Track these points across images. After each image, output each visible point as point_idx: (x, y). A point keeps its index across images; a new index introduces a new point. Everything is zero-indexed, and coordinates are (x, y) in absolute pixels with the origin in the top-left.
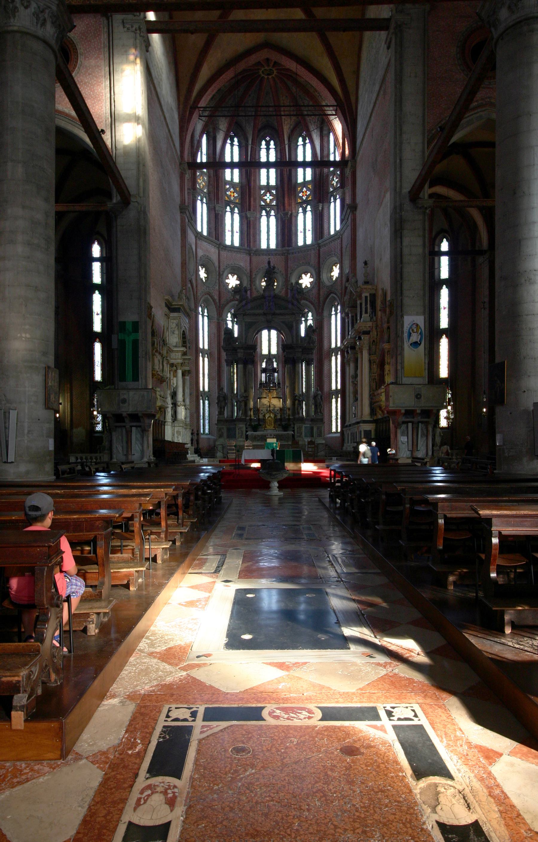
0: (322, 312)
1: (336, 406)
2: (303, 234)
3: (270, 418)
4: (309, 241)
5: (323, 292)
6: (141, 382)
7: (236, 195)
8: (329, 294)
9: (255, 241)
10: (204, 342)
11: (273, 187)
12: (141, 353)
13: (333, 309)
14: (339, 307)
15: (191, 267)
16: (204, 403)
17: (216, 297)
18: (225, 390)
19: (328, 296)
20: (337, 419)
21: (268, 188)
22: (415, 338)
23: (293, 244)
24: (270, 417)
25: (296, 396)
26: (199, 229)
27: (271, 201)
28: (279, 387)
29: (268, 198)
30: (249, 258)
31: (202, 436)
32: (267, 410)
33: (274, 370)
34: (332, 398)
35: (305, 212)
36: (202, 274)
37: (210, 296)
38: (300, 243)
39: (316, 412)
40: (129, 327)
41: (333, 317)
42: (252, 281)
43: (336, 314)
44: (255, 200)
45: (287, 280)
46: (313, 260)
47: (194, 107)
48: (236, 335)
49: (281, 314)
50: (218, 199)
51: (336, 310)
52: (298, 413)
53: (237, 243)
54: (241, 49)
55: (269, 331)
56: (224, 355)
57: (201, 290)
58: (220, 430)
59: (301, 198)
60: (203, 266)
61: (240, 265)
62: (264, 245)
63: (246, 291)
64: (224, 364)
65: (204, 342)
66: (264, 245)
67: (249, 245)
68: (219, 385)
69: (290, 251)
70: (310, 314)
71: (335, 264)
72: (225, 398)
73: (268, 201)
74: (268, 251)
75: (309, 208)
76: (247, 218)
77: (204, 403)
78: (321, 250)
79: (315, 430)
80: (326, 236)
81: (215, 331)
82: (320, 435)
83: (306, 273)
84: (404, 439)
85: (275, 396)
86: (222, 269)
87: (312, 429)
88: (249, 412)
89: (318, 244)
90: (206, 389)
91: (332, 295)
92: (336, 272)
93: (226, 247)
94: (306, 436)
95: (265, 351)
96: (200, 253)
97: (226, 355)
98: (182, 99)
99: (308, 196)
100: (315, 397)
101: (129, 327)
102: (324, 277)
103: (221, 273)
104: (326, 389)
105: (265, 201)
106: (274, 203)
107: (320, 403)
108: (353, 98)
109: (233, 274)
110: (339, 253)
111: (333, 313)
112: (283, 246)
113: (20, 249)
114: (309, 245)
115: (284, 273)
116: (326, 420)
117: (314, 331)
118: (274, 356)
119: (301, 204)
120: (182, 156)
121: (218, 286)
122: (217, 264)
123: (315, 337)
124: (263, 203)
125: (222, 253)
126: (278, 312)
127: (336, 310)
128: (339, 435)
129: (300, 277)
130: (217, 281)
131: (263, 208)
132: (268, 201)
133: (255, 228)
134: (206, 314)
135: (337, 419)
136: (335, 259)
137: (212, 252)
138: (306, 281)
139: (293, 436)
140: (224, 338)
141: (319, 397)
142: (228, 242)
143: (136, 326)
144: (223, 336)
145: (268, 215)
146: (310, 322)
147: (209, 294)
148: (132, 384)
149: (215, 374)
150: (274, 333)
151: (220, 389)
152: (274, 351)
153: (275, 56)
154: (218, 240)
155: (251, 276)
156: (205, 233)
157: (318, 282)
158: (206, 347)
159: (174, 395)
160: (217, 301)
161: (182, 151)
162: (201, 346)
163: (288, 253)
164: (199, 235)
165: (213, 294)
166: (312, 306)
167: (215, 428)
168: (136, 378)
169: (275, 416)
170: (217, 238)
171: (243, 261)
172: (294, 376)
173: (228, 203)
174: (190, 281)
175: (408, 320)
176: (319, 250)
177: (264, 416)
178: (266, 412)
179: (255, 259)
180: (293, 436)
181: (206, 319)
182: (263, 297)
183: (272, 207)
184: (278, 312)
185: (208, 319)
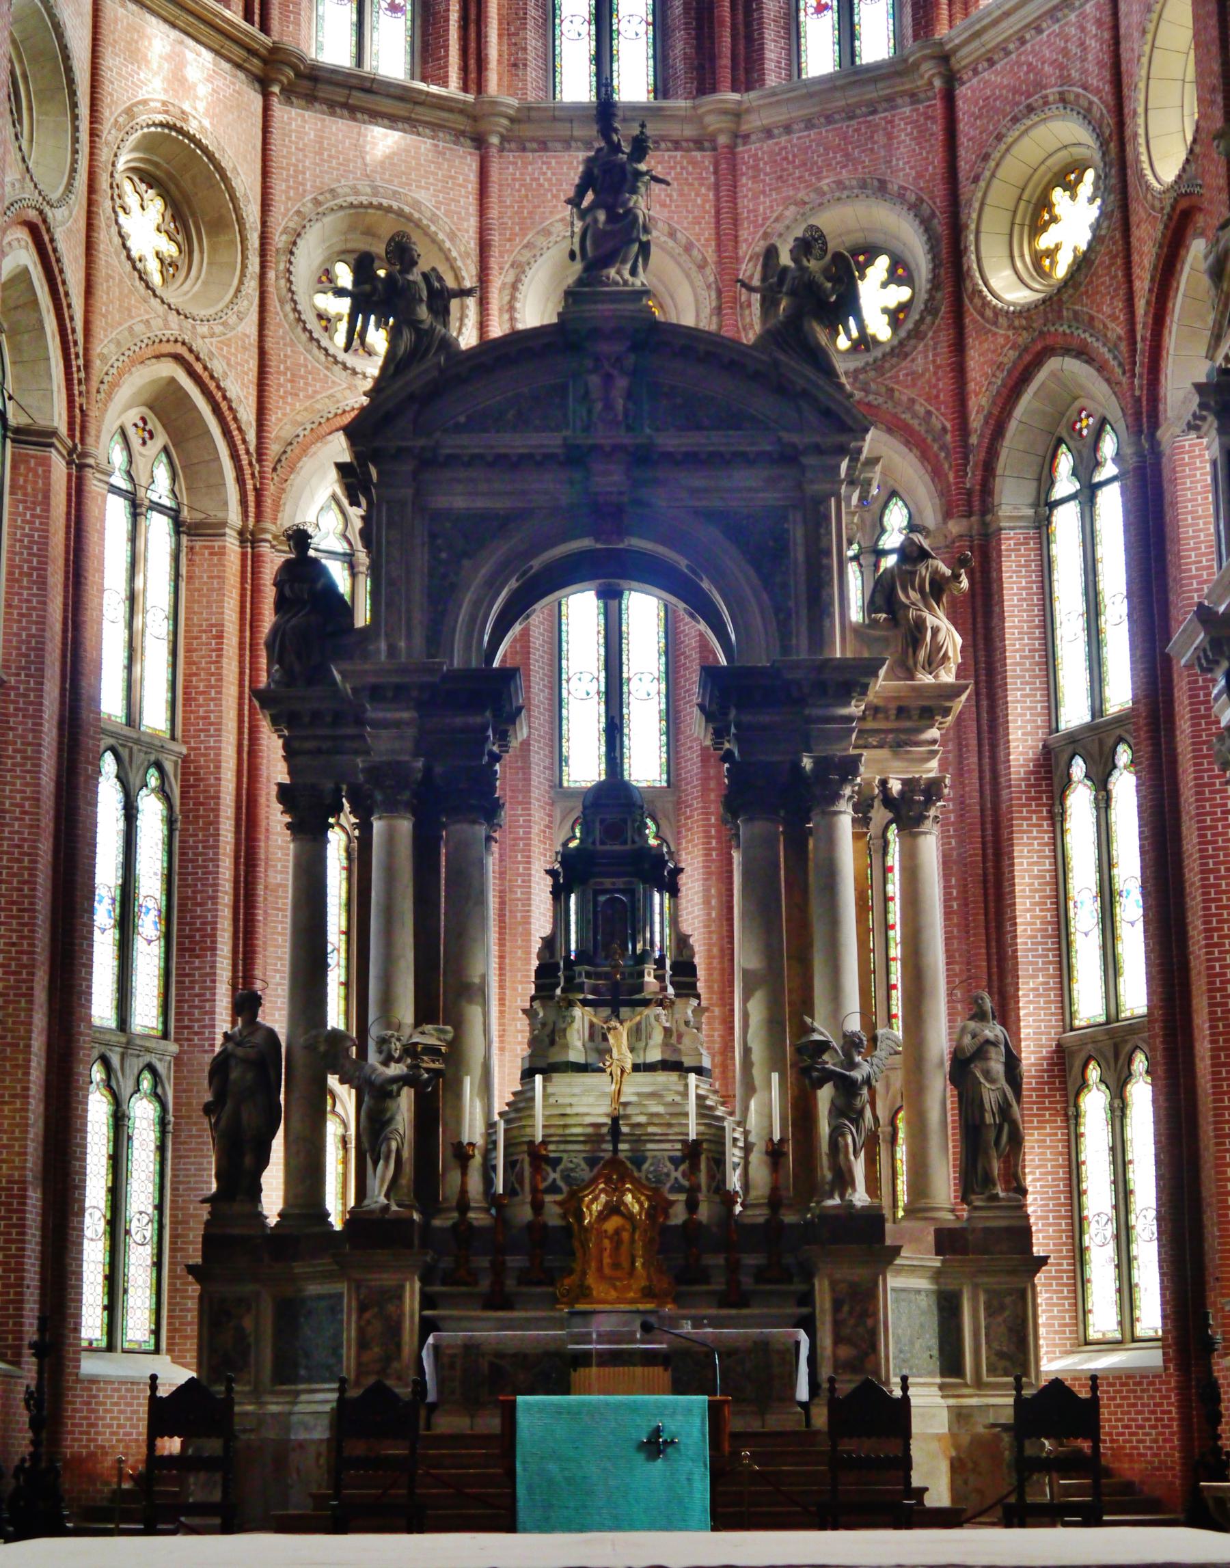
0: (986, 489)
2: (830, 18)
3: (613, 1223)
8: (1038, 361)
13: (1065, 463)
14: (1108, 446)
16: (119, 1120)
20: (1124, 1236)
24: (614, 1209)
25: (824, 1046)
30: (475, 166)
32: (592, 1162)
34: (1083, 1085)
37: (192, 373)
41: (1066, 520)
43: (1088, 494)
49: (693, 460)
51: (1086, 467)
52: (844, 1180)
55: (610, 597)
61: (416, 204)
64: (275, 818)
69: (753, 122)
71: (1066, 177)
77: (119, 1120)
78: (962, 91)
85: (654, 1055)
86: (281, 219)
88: (454, 1177)
91: (1053, 364)
97: (290, 754)
103: (279, 240)
107: (1004, 1110)
110: (1098, 78)
111: (1065, 484)
114: (877, 73)
115: (711, 255)
121: (254, 316)
126: (671, 441)
127: (1086, 467)
128: (1153, 1358)
130: (252, 286)
134: (160, 488)
135: (1124, 1236)
140: (275, 630)
141: (997, 1066)
154: (265, 28)
158: (155, 717)
160: (247, 414)
162: (111, 704)
165: (218, 367)
169: (659, 1207)
174: (33, 229)
176: (949, 98)
177: (573, 1206)
178: (585, 1173)
184: (671, 441)
185: (179, 527)
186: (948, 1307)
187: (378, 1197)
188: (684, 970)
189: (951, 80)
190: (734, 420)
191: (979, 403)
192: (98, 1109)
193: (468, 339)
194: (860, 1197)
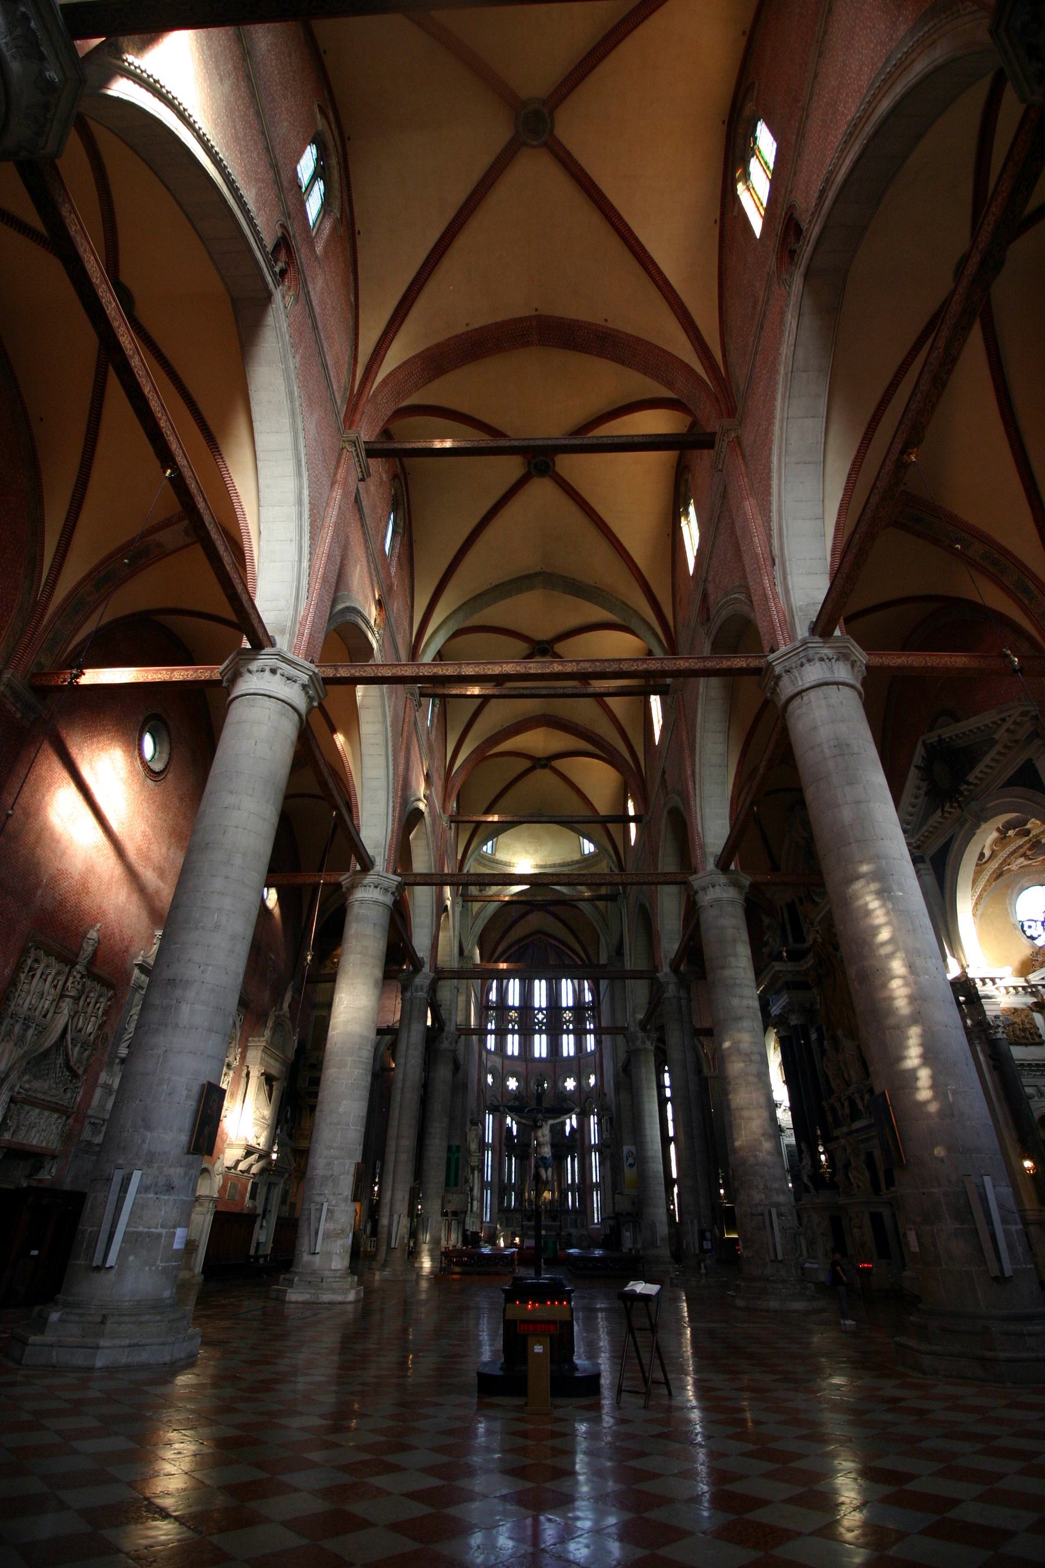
4: (572, 1054)
10: (489, 1138)
11: (544, 1009)
15: (483, 1073)
17: (500, 1098)
19: (586, 1100)
21: (540, 1009)
22: (631, 1161)
26: (489, 1047)
27: (543, 1019)
29: (540, 1016)
36: (490, 1079)
38: (565, 1054)
40: (454, 1149)
44: (530, 1019)
48: (515, 1133)
53: (516, 1053)
56: (504, 1148)
62: (537, 1055)
63: (523, 1098)
65: (489, 1138)
66: (537, 1055)
74: (540, 1059)
79: (579, 1220)
80: (584, 1053)
81: (497, 1126)
83: (570, 1077)
84: (628, 1234)
87: (576, 1220)
89: (579, 1057)
92: (592, 1080)
93: (508, 1057)
96: (489, 1064)
101: (454, 1149)
102: (584, 1082)
104: (588, 1182)
105: (538, 1019)
106: (545, 1021)
109: (513, 1077)
112: (552, 1056)
119: (565, 1023)
120: (481, 1003)
122: (501, 1071)
123: (578, 1136)
124: (536, 1021)
125: (505, 1061)
129: (565, 1081)
136: (590, 1069)
137: (497, 1061)
138: (570, 1084)
139: (560, 1227)
142: (510, 1053)
143: (458, 1147)
144: (504, 1134)
146: (575, 1124)
147: (494, 1096)
156: (493, 1049)
157: (579, 1086)
159: (472, 1189)
161: (482, 1000)
164: (489, 1052)
168: (456, 1185)
171: (520, 1067)
175: (626, 1149)
180: (560, 1227)
191: (582, 1101)
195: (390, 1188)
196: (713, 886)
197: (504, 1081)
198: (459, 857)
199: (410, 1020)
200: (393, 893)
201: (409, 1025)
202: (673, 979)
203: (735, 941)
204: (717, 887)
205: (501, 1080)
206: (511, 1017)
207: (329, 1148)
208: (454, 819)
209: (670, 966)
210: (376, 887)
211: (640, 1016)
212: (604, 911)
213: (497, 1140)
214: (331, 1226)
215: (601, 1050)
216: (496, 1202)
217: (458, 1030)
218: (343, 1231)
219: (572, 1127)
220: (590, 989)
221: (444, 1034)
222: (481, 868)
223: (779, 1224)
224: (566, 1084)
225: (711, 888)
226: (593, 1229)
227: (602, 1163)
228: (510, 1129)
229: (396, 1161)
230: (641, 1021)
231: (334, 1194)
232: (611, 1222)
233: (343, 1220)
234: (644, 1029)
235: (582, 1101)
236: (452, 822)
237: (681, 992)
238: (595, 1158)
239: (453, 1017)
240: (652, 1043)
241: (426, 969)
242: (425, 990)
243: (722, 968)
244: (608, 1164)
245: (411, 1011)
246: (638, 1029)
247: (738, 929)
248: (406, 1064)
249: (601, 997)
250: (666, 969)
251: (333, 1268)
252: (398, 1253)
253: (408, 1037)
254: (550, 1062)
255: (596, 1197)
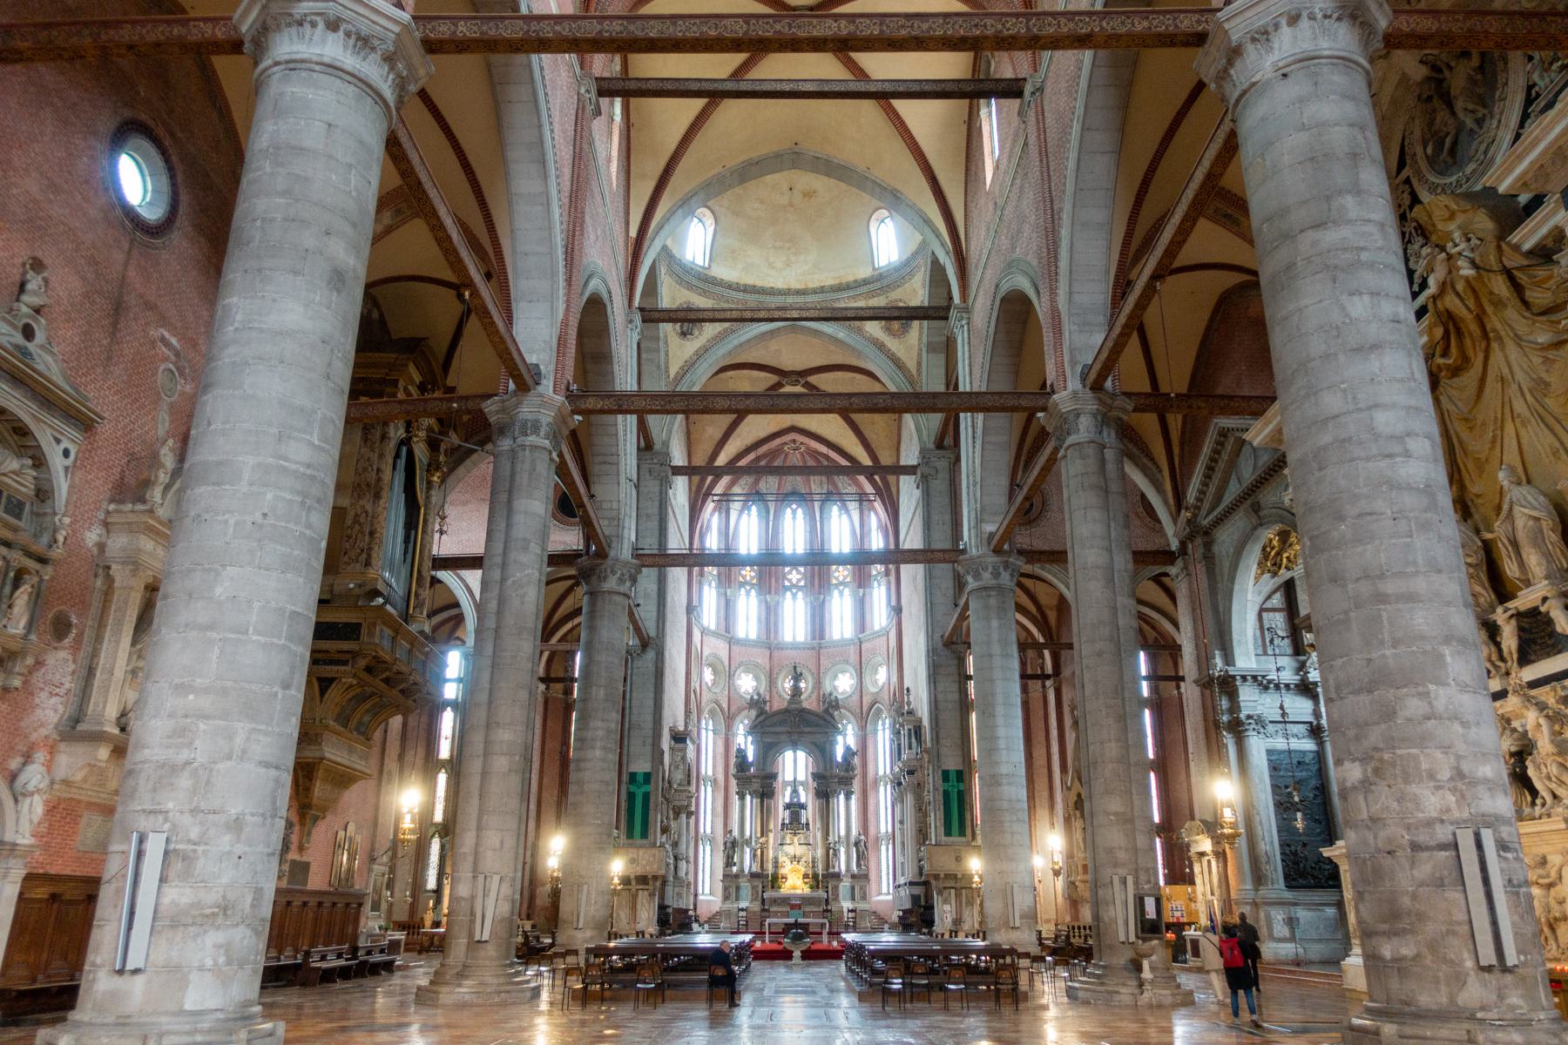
1: (885, 855)
5: (867, 700)
6: (651, 838)
7: (753, 574)
9: (776, 632)
12: (652, 805)
17: (725, 705)
18: (736, 833)
23: (827, 637)
27: (799, 580)
28: (808, 829)
31: (701, 897)
33: (803, 807)
35: (841, 593)
36: (708, 675)
39: (858, 865)
41: (880, 733)
42: (772, 682)
45: (818, 683)
46: (854, 658)
47: (708, 494)
50: (730, 582)
51: (884, 724)
54: (762, 434)
56: (733, 783)
57: (706, 697)
58: (726, 889)
59: (837, 578)
60: (710, 665)
63: (765, 702)
67: (768, 637)
68: (726, 824)
70: (850, 727)
72: (734, 844)
73: (794, 581)
74: (795, 646)
75: (847, 591)
76: (766, 602)
80: (868, 632)
82: (864, 898)
86: (733, 669)
90: (708, 831)
92: (882, 675)
93: (738, 642)
94: (844, 899)
95: (789, 777)
96: (706, 652)
98: (694, 488)
99: (845, 577)
100: (857, 844)
104: (872, 831)
105: (790, 580)
106: (802, 583)
108: (894, 489)
109: (747, 671)
111: (880, 727)
113: (598, 753)
116: (873, 876)
117: (854, 754)
118: (802, 784)
119: (837, 586)
122: (727, 663)
123: (856, 761)
124: (787, 583)
127: (884, 724)
129: (835, 677)
131: (786, 589)
132: (794, 581)
133: (776, 615)
134: (711, 727)
136: (880, 658)
139: (827, 900)
144: (733, 760)
145: (794, 595)
147: (717, 702)
148: (640, 842)
149: (720, 809)
150: (801, 755)
151: (727, 831)
152: (801, 777)
153: (800, 438)
155: (770, 676)
163: (820, 648)
164: (705, 631)
166: (852, 718)
167: (719, 887)
168: (644, 835)
170: (727, 630)
172: (826, 815)
173: (742, 585)
179: (776, 654)
180: (827, 900)
181: (711, 733)
182: (786, 711)
183: (800, 588)
186: (853, 888)
187: (754, 869)
188: (808, 824)
189: (861, 643)
190: (817, 725)
191: (865, 709)
192: (701, 848)
193: (767, 708)
194: (837, 870)
195: (473, 824)
196: (1294, 20)
197: (730, 676)
198: (633, 233)
199: (510, 492)
200: (389, 59)
201: (510, 501)
202: (1090, 404)
203: (1354, 156)
204: (1304, 23)
205: (727, 675)
206: (744, 577)
207: (182, 689)
208: (605, 85)
209: (1083, 379)
210: (333, 25)
211: (990, 528)
212: (914, 372)
213: (720, 769)
214: (178, 895)
215: (899, 624)
216: (720, 864)
217: (637, 556)
218: (225, 909)
219: (848, 749)
220: (881, 526)
221: (609, 562)
222: (665, 210)
223: (1502, 870)
224: (836, 683)
225: (1285, 30)
226: (879, 901)
227: (898, 799)
228: (741, 754)
229: (485, 774)
230: (992, 535)
231: (195, 811)
232: (918, 890)
233: (225, 880)
234: (997, 551)
235: (865, 709)
236: (601, 93)
237: (1105, 434)
238: (884, 797)
239: (626, 535)
240: (1012, 575)
241: (547, 387)
242: (542, 433)
243: (1319, 225)
244: (909, 799)
245: (513, 475)
246: (984, 550)
247: (1362, 128)
248: (503, 580)
249: (902, 537)
250: (1074, 384)
251: (188, 1007)
252: (491, 950)
253: (509, 526)
254: (813, 648)
255: (885, 855)
